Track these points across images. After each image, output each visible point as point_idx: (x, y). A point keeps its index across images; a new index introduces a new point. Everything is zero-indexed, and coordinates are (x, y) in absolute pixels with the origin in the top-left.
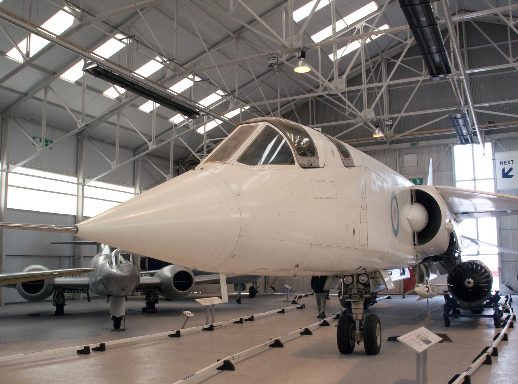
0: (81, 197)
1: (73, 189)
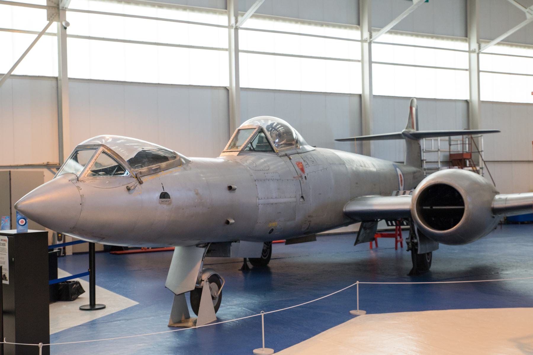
0: (476, 73)
1: (462, 60)
